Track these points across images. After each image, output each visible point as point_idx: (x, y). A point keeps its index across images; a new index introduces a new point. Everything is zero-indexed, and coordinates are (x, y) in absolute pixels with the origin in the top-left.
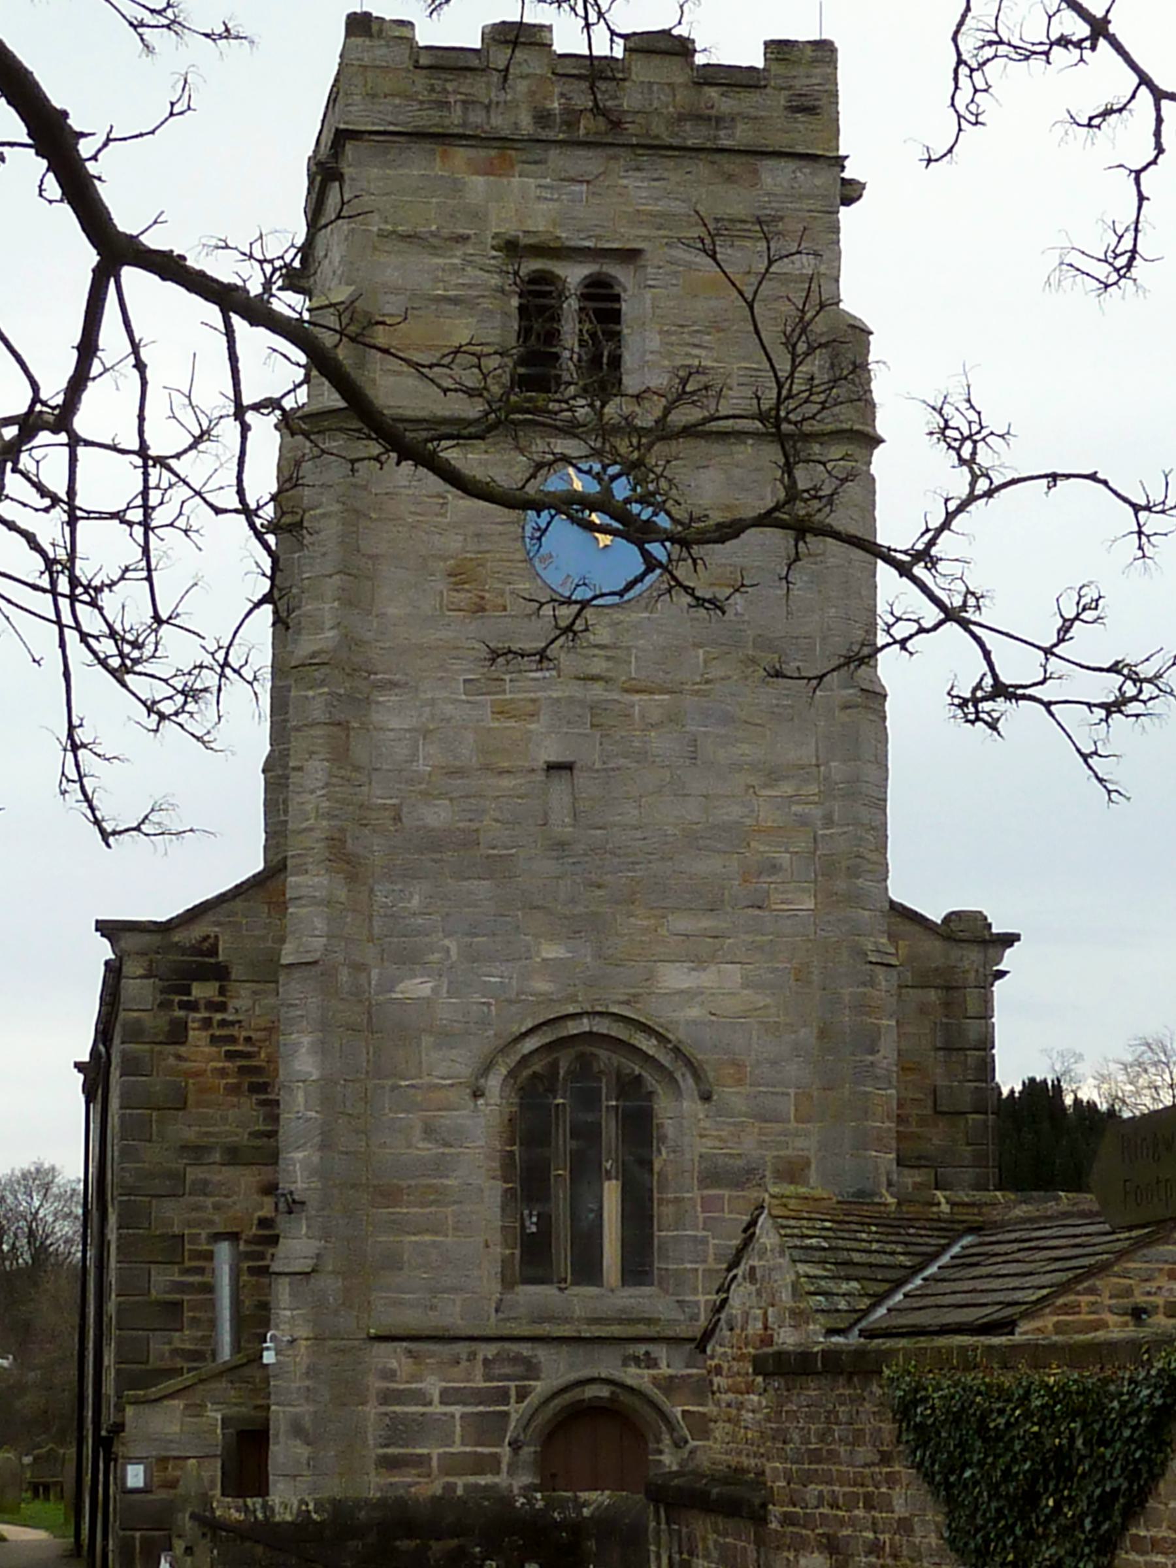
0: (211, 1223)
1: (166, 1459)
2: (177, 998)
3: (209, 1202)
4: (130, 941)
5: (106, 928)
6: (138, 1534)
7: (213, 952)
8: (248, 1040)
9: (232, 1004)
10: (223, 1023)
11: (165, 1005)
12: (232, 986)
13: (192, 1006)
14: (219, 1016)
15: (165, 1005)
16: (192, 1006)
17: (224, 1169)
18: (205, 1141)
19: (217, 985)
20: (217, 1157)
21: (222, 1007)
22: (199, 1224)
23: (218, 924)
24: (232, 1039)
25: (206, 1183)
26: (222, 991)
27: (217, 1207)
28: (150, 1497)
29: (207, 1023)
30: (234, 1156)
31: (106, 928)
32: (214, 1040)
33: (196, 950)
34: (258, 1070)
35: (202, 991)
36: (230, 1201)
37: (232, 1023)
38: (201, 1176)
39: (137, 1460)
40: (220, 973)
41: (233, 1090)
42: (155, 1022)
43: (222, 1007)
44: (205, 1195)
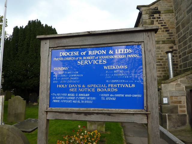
0: (161, 54)
1: (172, 96)
2: (152, 17)
3: (160, 50)
4: (143, 9)
5: (138, 8)
6: (167, 114)
7: (157, 9)
8: (165, 23)
9: (161, 17)
10: (160, 21)
11: (150, 18)
12: (161, 14)
13: (155, 18)
14: (159, 19)
15: (150, 18)
16: (155, 18)
17: (162, 44)
18: (158, 40)
19: (159, 14)
20: (161, 42)
21: (160, 18)
22: (159, 54)
23: (158, 5)
24: (162, 23)
25: (159, 47)
26: (160, 15)
27: (162, 51)
28: (169, 106)
29: (157, 21)
30: (164, 42)
31: (138, 8)
32: (159, 23)
33: (154, 9)
34: (167, 28)
35: (156, 16)
36: (164, 50)
37: (162, 21)
38: (158, 46)
39: (166, 97)
40: (159, 12)
41: (163, 31)
42: (148, 21)
43: (160, 18)
44: (159, 49)
